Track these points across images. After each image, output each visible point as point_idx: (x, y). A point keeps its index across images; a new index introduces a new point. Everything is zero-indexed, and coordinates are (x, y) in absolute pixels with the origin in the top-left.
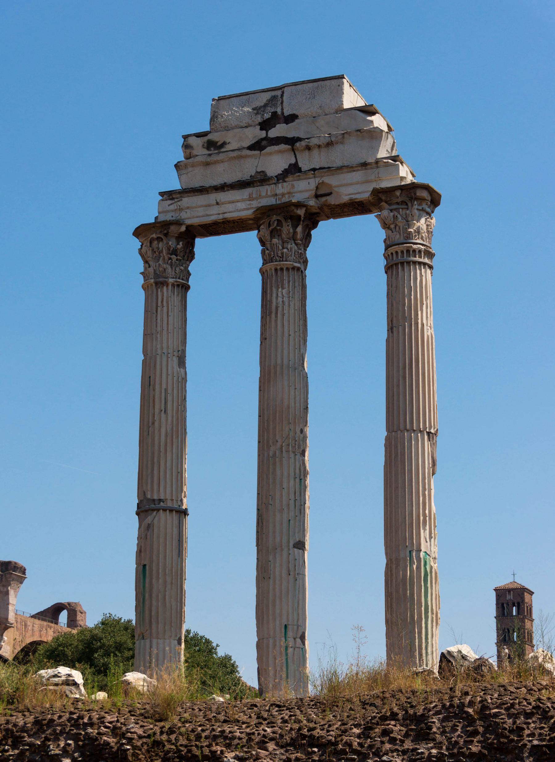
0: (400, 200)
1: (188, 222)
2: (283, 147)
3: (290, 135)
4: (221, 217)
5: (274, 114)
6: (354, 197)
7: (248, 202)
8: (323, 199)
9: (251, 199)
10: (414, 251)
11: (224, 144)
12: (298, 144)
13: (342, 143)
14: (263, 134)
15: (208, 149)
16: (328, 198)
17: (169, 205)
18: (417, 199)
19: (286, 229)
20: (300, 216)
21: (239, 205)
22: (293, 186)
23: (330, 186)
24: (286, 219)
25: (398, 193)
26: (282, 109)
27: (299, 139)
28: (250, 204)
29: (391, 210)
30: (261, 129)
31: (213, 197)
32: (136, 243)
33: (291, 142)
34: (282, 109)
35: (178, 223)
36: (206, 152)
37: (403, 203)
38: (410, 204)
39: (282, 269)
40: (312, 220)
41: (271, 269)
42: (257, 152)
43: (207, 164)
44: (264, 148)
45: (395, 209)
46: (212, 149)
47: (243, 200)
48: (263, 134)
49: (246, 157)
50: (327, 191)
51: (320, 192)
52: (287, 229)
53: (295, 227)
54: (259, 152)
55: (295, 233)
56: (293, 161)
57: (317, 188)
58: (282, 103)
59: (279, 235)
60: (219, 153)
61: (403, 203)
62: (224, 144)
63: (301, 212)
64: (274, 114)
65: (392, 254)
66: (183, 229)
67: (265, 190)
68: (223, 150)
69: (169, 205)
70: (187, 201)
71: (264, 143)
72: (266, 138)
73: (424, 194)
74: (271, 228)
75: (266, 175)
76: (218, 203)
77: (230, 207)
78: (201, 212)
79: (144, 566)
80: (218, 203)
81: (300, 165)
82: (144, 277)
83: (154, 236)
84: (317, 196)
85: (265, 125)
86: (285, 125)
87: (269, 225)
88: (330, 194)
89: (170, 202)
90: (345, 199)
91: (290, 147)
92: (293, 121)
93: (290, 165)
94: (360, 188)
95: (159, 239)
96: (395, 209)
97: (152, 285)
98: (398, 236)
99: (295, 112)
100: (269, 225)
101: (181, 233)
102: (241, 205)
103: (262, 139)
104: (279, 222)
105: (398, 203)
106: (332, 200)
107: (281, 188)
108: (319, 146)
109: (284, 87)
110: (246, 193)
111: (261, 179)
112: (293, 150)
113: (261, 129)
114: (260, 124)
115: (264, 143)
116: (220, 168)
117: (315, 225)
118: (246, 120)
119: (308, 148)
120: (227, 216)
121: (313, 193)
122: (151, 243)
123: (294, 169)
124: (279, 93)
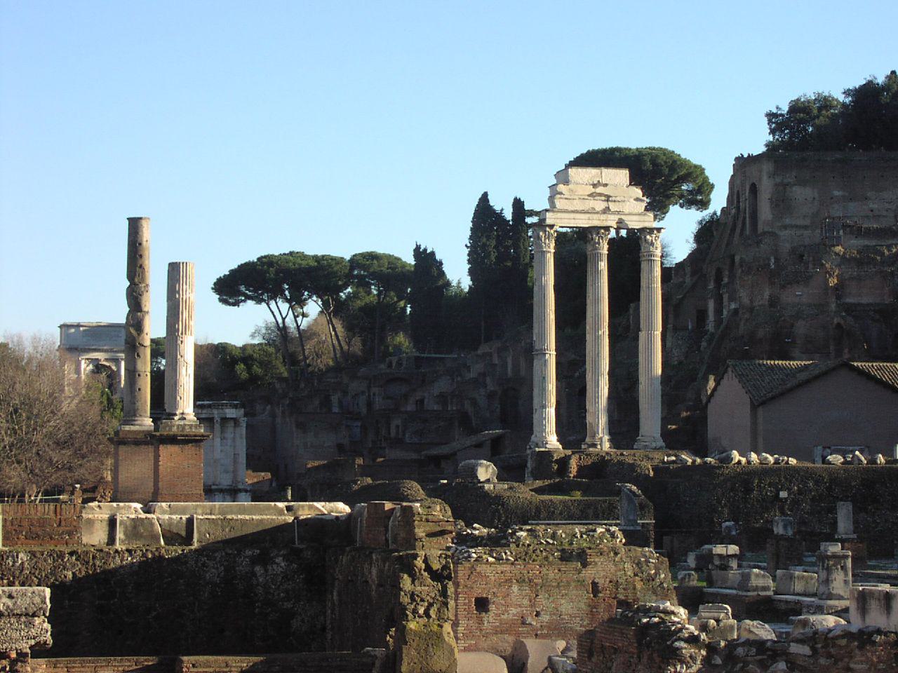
2: (603, 198)
9: (589, 219)
31: (572, 215)
33: (608, 197)
48: (593, 190)
62: (575, 192)
64: (599, 181)
67: (595, 216)
70: (559, 215)
71: (594, 194)
72: (595, 193)
77: (580, 222)
79: (544, 378)
81: (610, 208)
85: (594, 186)
107: (603, 217)
111: (592, 211)
115: (594, 194)
123: (606, 210)
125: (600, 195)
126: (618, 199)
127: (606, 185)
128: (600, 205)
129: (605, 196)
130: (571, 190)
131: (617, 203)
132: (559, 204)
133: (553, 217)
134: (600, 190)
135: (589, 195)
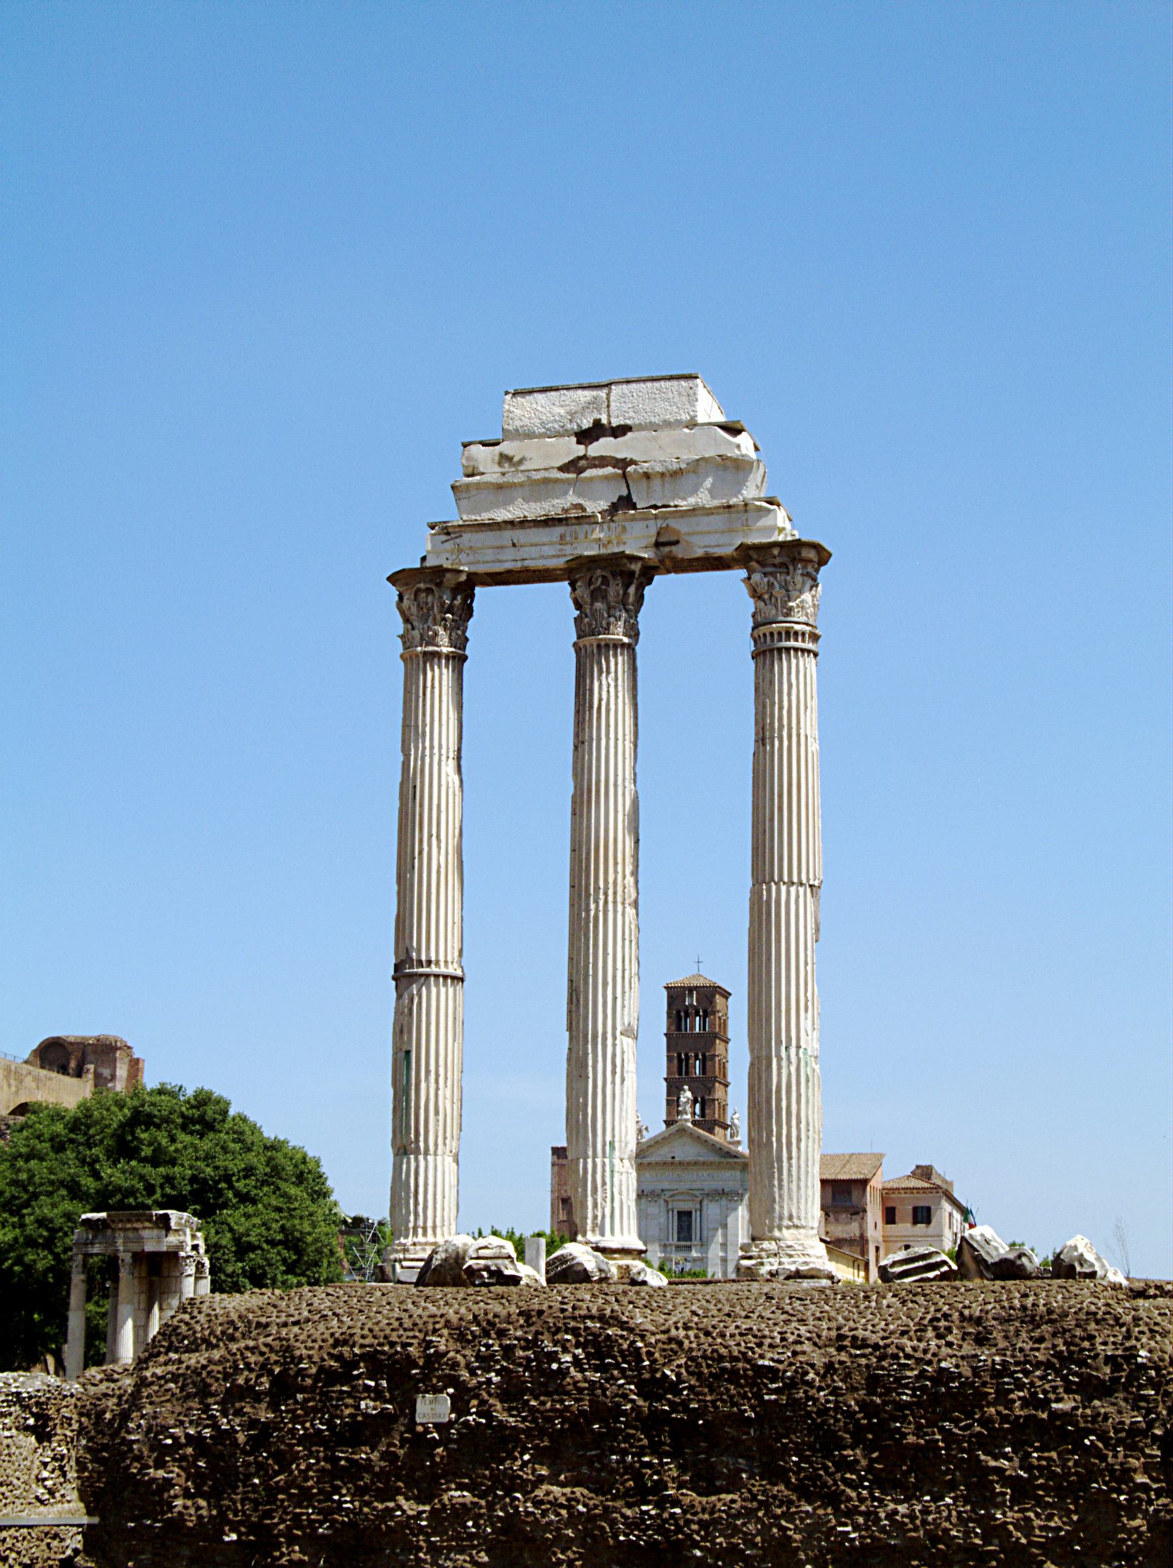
0: (777, 561)
2: (609, 470)
3: (620, 456)
4: (519, 565)
5: (597, 423)
6: (711, 550)
7: (560, 547)
8: (667, 549)
10: (796, 633)
12: (630, 469)
13: (694, 472)
14: (580, 450)
15: (500, 464)
16: (674, 548)
18: (802, 560)
19: (608, 588)
20: (633, 573)
21: (546, 550)
23: (678, 533)
24: (614, 575)
25: (776, 551)
27: (632, 462)
28: (561, 550)
29: (765, 574)
30: (579, 442)
31: (508, 535)
32: (393, 592)
34: (609, 416)
36: (497, 469)
37: (783, 565)
38: (791, 568)
39: (607, 646)
40: (648, 573)
41: (592, 645)
42: (572, 476)
45: (771, 574)
46: (506, 465)
47: (551, 544)
48: (580, 450)
49: (557, 481)
50: (673, 538)
51: (662, 540)
52: (614, 589)
53: (626, 587)
54: (574, 476)
55: (626, 594)
56: (625, 493)
57: (658, 534)
58: (608, 406)
59: (604, 598)
60: (517, 471)
61: (783, 565)
63: (636, 567)
64: (597, 423)
65: (765, 635)
66: (463, 578)
68: (522, 468)
72: (584, 457)
73: (812, 554)
74: (592, 587)
76: (514, 545)
77: (534, 552)
78: (490, 555)
81: (635, 499)
82: (404, 643)
83: (422, 586)
84: (658, 545)
85: (585, 436)
86: (611, 439)
87: (590, 583)
88: (676, 543)
89: (445, 538)
90: (699, 553)
91: (620, 471)
92: (624, 434)
93: (620, 498)
94: (723, 539)
95: (429, 591)
96: (771, 574)
97: (417, 656)
98: (774, 612)
99: (628, 422)
100: (590, 583)
101: (460, 584)
102: (548, 550)
103: (580, 458)
104: (605, 581)
105: (774, 565)
106: (679, 552)
109: (611, 384)
113: (579, 442)
114: (577, 434)
117: (650, 581)
121: (653, 540)
122: (416, 595)
124: (602, 393)
125: (602, 461)
127: (620, 431)
134: (603, 447)
135: (563, 469)
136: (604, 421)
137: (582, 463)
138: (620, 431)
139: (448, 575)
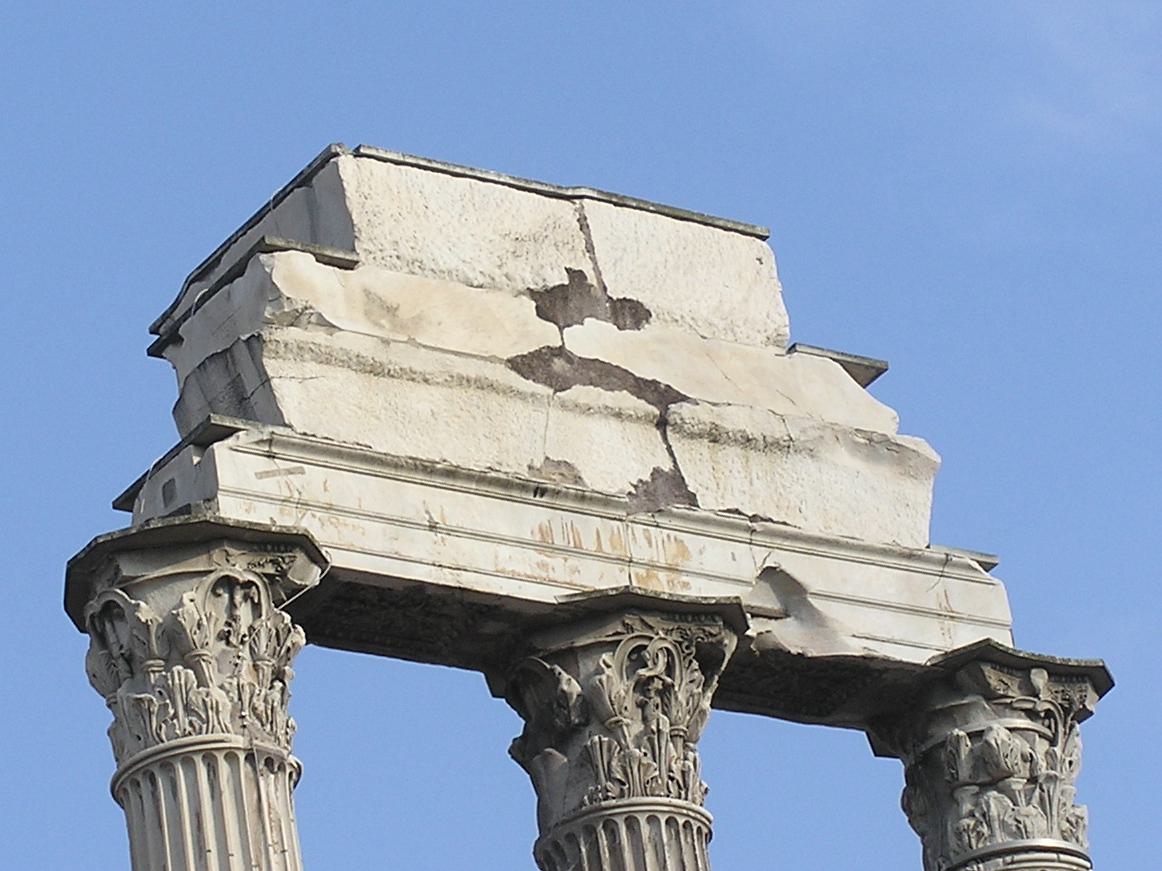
0: (1042, 707)
1: (337, 559)
7: (535, 556)
9: (544, 545)
11: (418, 320)
13: (811, 453)
14: (547, 334)
17: (260, 475)
22: (683, 551)
26: (596, 268)
28: (542, 565)
30: (541, 313)
31: (415, 498)
33: (662, 396)
34: (596, 268)
35: (315, 555)
43: (375, 370)
44: (560, 384)
48: (547, 334)
54: (551, 391)
56: (667, 466)
58: (590, 248)
66: (314, 577)
67: (590, 528)
69: (260, 475)
70: (317, 480)
72: (560, 352)
75: (578, 479)
78: (375, 536)
80: (433, 527)
85: (554, 303)
89: (264, 464)
90: (855, 648)
105: (1032, 714)
106: (790, 636)
108: (747, 441)
110: (530, 518)
112: (662, 424)
116: (421, 400)
118: (484, 265)
119: (714, 436)
120: (468, 581)
123: (665, 493)
126: (735, 420)
127: (630, 313)
128: (615, 452)
129: (644, 388)
130: (381, 308)
131: (732, 454)
132: (300, 390)
133: (270, 486)
134: (591, 338)
135: (523, 365)
136: (592, 279)
137: (558, 364)
138: (630, 313)
139: (301, 558)
